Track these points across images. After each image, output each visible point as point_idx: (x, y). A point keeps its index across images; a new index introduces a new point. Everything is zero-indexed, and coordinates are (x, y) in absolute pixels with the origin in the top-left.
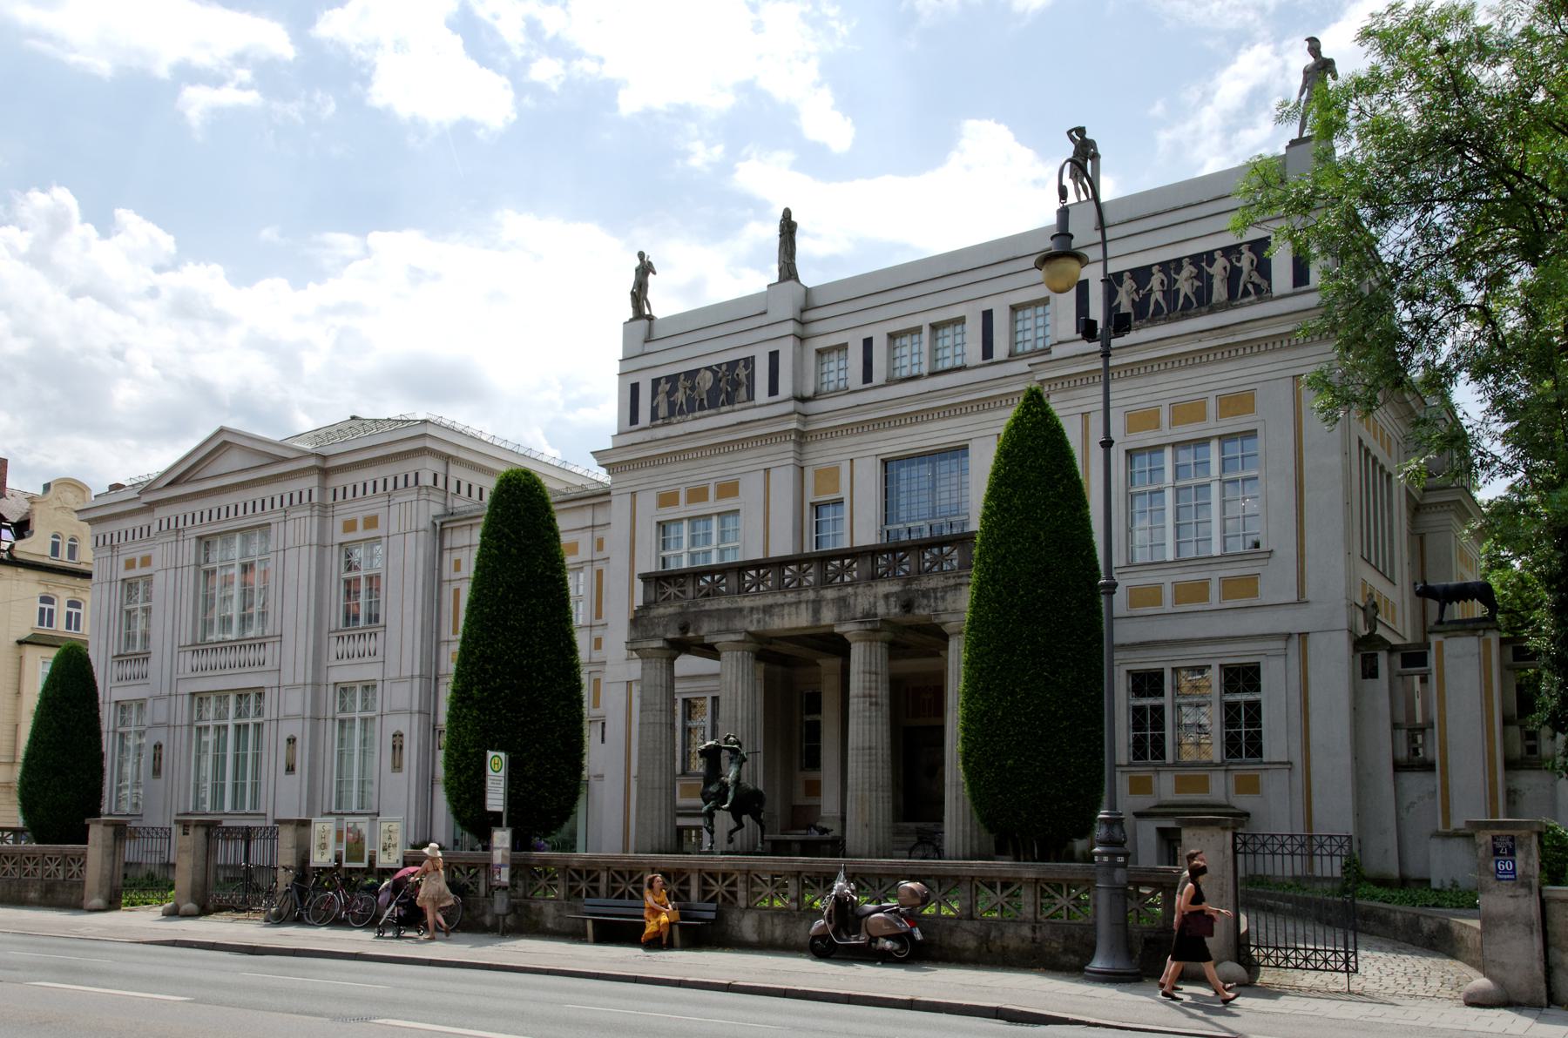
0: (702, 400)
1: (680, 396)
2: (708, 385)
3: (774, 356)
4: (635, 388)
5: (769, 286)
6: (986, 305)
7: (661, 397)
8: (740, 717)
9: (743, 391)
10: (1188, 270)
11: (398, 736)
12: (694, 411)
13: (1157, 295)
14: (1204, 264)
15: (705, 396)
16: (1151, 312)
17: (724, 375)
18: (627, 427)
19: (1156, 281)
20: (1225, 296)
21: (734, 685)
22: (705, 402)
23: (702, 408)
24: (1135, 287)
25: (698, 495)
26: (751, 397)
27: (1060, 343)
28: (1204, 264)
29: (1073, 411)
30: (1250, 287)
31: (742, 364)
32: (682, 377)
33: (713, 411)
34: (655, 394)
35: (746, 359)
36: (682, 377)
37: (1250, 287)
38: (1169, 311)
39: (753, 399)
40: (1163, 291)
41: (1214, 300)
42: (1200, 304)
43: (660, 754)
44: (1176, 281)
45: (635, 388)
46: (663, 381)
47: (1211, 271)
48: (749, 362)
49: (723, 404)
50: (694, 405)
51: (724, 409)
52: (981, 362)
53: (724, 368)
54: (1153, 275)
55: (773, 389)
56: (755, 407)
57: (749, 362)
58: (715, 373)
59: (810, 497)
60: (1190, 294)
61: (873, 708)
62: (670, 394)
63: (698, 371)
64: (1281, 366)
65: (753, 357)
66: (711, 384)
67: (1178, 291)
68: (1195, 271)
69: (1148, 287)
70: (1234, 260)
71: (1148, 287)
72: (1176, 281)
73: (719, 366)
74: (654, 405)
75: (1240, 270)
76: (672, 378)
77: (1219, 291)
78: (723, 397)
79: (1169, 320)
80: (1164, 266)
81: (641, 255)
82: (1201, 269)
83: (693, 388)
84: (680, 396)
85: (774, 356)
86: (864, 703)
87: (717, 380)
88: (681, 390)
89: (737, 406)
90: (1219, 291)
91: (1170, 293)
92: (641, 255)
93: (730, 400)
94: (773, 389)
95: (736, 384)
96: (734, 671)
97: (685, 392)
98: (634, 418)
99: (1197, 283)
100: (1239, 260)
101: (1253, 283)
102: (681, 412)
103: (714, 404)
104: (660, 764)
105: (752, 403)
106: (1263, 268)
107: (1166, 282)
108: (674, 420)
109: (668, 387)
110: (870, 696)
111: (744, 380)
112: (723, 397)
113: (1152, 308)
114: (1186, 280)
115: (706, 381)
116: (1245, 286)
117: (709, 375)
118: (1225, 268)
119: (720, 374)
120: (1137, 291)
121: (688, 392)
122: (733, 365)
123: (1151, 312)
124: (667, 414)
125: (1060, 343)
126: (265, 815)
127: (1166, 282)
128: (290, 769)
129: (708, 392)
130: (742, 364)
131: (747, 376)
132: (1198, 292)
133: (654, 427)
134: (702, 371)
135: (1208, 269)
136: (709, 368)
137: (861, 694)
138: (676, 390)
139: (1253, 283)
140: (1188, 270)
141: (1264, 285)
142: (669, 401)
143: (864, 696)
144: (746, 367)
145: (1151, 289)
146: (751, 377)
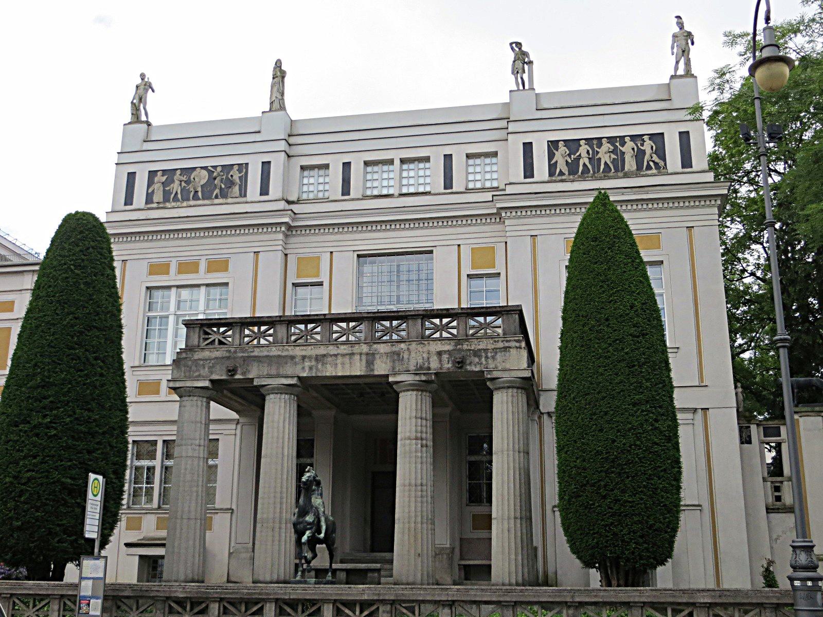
0: (196, 192)
1: (176, 187)
2: (203, 182)
3: (266, 165)
9: (236, 189)
10: (606, 146)
12: (188, 200)
13: (585, 160)
14: (618, 144)
15: (199, 189)
17: (219, 175)
18: (122, 207)
19: (583, 149)
22: (200, 194)
26: (243, 193)
28: (618, 144)
31: (236, 168)
38: (594, 172)
39: (245, 196)
41: (626, 169)
42: (617, 170)
44: (598, 153)
47: (623, 149)
49: (216, 197)
53: (219, 169)
55: (264, 191)
67: (600, 159)
72: (598, 153)
74: (150, 191)
77: (630, 164)
79: (594, 178)
84: (176, 187)
85: (266, 165)
88: (177, 182)
89: (230, 200)
90: (630, 164)
93: (224, 194)
94: (264, 191)
95: (231, 183)
97: (181, 185)
99: (613, 156)
100: (642, 145)
102: (175, 199)
105: (243, 199)
108: (168, 205)
109: (164, 179)
111: (238, 181)
118: (633, 149)
119: (215, 174)
120: (569, 155)
121: (183, 184)
124: (161, 200)
127: (591, 152)
129: (202, 186)
130: (236, 168)
138: (173, 181)
140: (606, 146)
142: (164, 190)
144: (240, 171)
145: (580, 155)
146: (244, 179)
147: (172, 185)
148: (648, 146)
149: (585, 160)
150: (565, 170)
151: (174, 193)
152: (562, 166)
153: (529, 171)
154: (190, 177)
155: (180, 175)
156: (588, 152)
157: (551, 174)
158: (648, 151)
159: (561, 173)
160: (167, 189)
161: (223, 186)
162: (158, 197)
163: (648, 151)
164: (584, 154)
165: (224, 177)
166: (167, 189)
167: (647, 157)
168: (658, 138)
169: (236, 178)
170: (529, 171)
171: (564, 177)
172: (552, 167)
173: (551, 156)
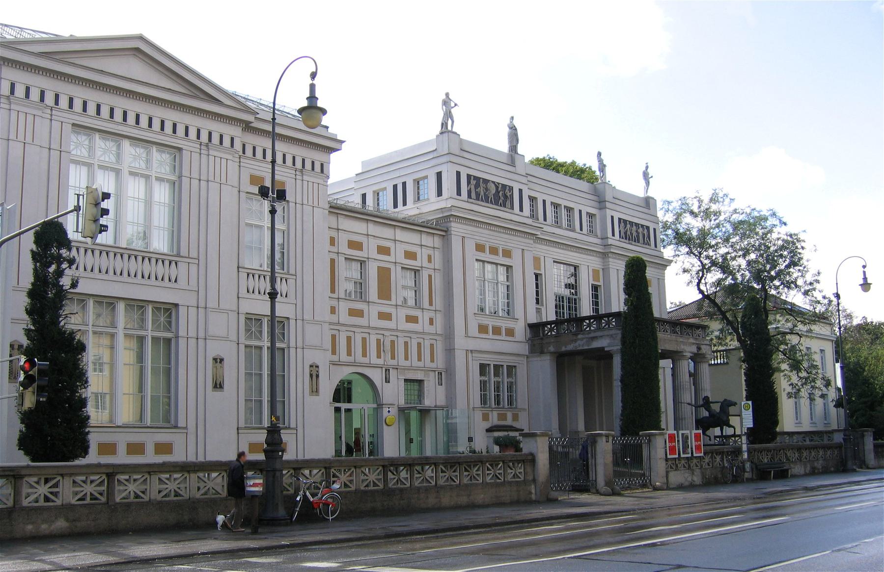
7: (473, 187)
11: (314, 367)
25: (494, 251)
26: (512, 208)
34: (469, 183)
58: (497, 187)
64: (656, 273)
73: (499, 183)
81: (447, 95)
83: (487, 189)
87: (497, 192)
92: (447, 95)
103: (497, 204)
117: (493, 186)
122: (504, 186)
126: (186, 428)
128: (218, 386)
129: (494, 195)
133: (468, 202)
136: (494, 182)
149: (629, 233)
152: (622, 234)
157: (620, 237)
162: (473, 195)
166: (477, 190)
169: (508, 194)
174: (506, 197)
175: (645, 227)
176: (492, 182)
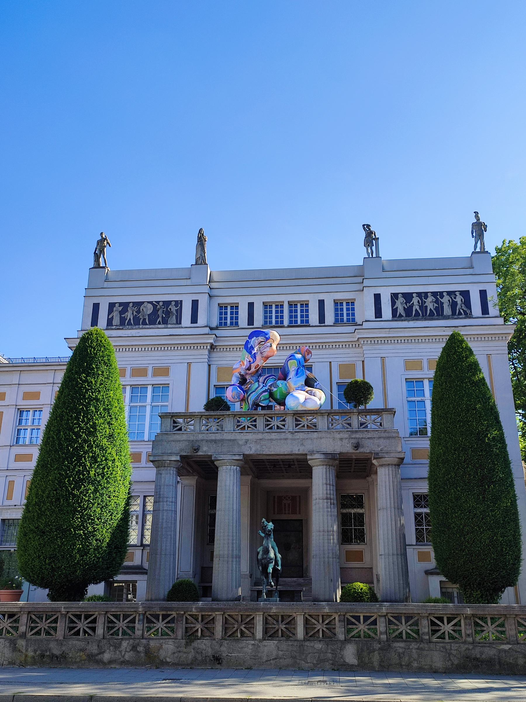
0: (145, 319)
1: (129, 315)
4: (96, 307)
5: (192, 265)
6: (321, 297)
8: (235, 508)
10: (430, 298)
13: (416, 307)
14: (438, 297)
15: (147, 317)
16: (413, 315)
17: (161, 307)
19: (415, 300)
20: (450, 313)
21: (231, 488)
23: (144, 323)
24: (405, 301)
26: (179, 321)
27: (366, 321)
28: (438, 297)
29: (377, 355)
30: (462, 311)
31: (173, 303)
32: (131, 305)
33: (163, 326)
35: (176, 302)
36: (131, 305)
37: (462, 311)
38: (423, 316)
39: (180, 323)
40: (419, 306)
42: (438, 315)
43: (171, 531)
44: (425, 302)
45: (96, 307)
46: (117, 305)
48: (179, 304)
49: (159, 323)
50: (137, 322)
51: (160, 326)
52: (318, 324)
53: (161, 304)
54: (413, 297)
55: (194, 319)
56: (182, 328)
57: (179, 304)
58: (155, 306)
59: (214, 382)
60: (432, 309)
61: (332, 506)
62: (121, 313)
63: (143, 303)
65: (181, 301)
66: (151, 311)
67: (426, 307)
68: (435, 299)
69: (412, 303)
70: (453, 298)
71: (412, 303)
72: (425, 302)
73: (158, 302)
74: (110, 317)
75: (456, 303)
76: (125, 306)
77: (447, 310)
78: (160, 319)
80: (419, 294)
82: (437, 299)
83: (138, 312)
84: (129, 315)
86: (327, 503)
89: (169, 326)
90: (447, 310)
91: (423, 307)
93: (165, 322)
94: (194, 319)
96: (232, 478)
97: (133, 313)
98: (94, 322)
99: (436, 305)
100: (455, 298)
101: (462, 309)
102: (129, 323)
104: (171, 538)
106: (467, 303)
107: (420, 302)
109: (121, 308)
110: (331, 499)
111: (175, 312)
112: (160, 319)
113: (414, 313)
114: (430, 302)
115: (149, 309)
116: (459, 311)
117: (150, 306)
118: (449, 301)
119: (158, 307)
120: (406, 303)
121: (135, 313)
122: (167, 303)
123: (413, 315)
125: (366, 321)
127: (420, 302)
130: (173, 303)
131: (177, 311)
132: (436, 309)
134: (145, 304)
135: (441, 300)
136: (151, 303)
137: (325, 498)
139: (462, 309)
140: (430, 298)
141: (468, 312)
142: (121, 317)
143: (327, 499)
144: (176, 305)
147: (127, 313)
148: (459, 299)
149: (416, 307)
150: (403, 314)
151: (128, 319)
152: (401, 310)
153: (378, 313)
154: (139, 308)
155: (133, 306)
156: (418, 302)
158: (459, 302)
159: (401, 316)
160: (122, 316)
161: (164, 316)
162: (116, 321)
163: (459, 302)
164: (416, 303)
165: (165, 309)
166: (122, 316)
167: (458, 307)
168: (466, 294)
169: (173, 309)
170: (378, 313)
171: (403, 318)
172: (394, 312)
173: (393, 303)
174: (168, 313)
175: (457, 293)
176: (148, 302)
